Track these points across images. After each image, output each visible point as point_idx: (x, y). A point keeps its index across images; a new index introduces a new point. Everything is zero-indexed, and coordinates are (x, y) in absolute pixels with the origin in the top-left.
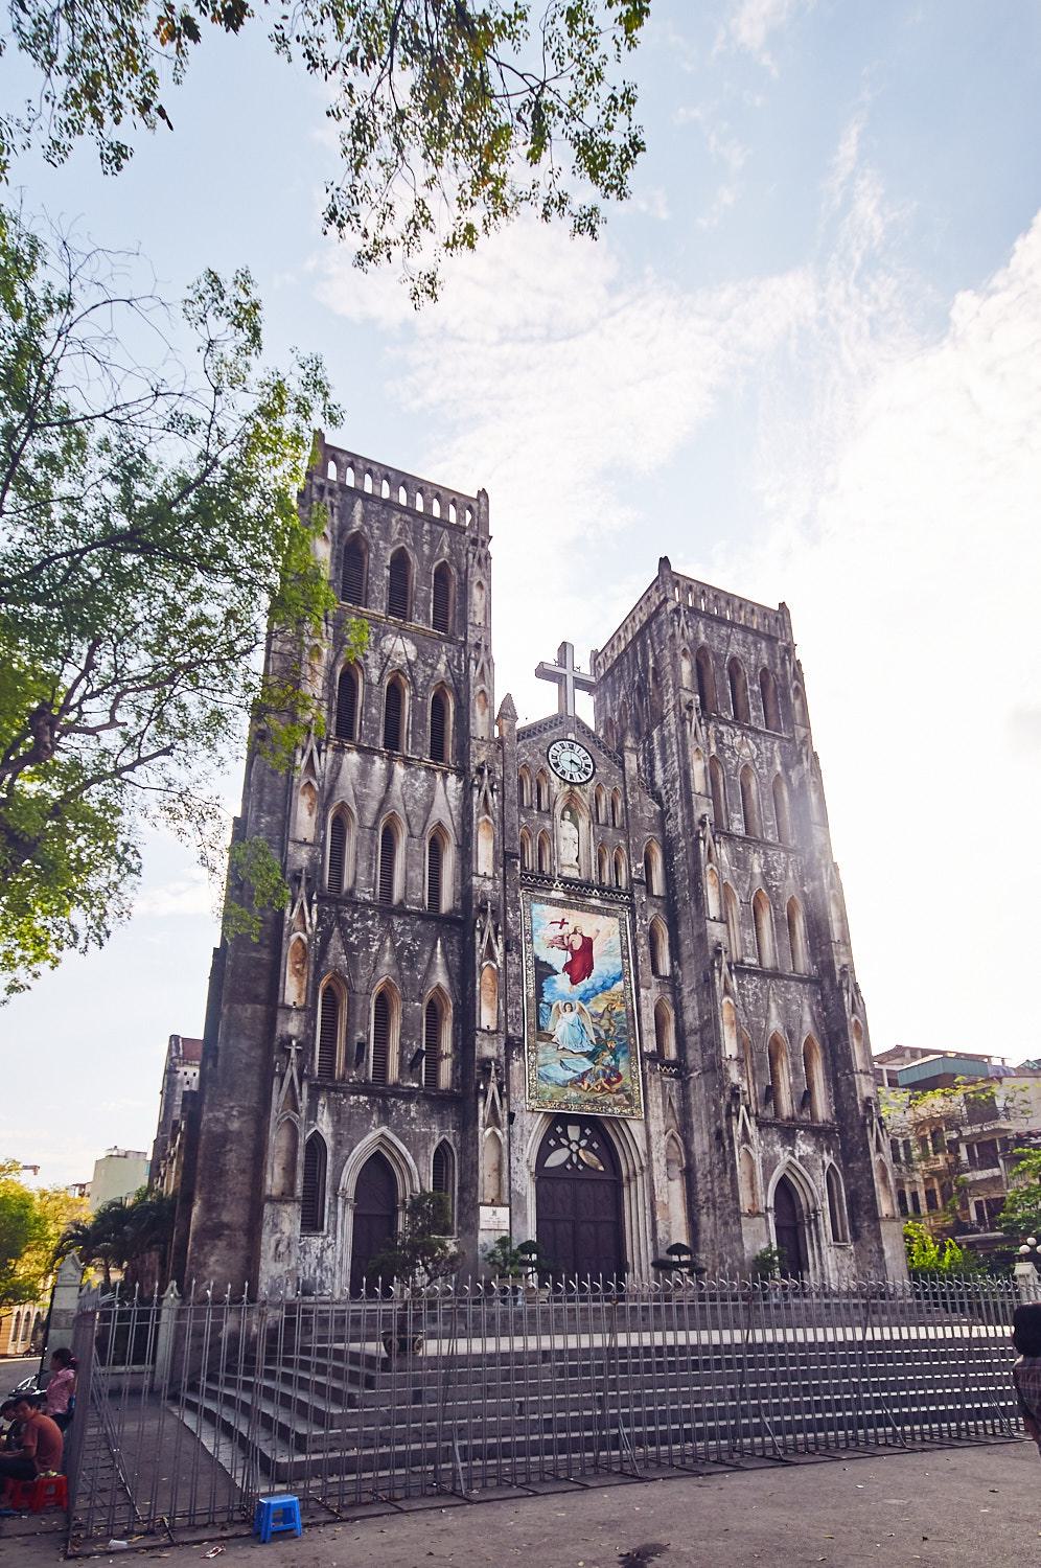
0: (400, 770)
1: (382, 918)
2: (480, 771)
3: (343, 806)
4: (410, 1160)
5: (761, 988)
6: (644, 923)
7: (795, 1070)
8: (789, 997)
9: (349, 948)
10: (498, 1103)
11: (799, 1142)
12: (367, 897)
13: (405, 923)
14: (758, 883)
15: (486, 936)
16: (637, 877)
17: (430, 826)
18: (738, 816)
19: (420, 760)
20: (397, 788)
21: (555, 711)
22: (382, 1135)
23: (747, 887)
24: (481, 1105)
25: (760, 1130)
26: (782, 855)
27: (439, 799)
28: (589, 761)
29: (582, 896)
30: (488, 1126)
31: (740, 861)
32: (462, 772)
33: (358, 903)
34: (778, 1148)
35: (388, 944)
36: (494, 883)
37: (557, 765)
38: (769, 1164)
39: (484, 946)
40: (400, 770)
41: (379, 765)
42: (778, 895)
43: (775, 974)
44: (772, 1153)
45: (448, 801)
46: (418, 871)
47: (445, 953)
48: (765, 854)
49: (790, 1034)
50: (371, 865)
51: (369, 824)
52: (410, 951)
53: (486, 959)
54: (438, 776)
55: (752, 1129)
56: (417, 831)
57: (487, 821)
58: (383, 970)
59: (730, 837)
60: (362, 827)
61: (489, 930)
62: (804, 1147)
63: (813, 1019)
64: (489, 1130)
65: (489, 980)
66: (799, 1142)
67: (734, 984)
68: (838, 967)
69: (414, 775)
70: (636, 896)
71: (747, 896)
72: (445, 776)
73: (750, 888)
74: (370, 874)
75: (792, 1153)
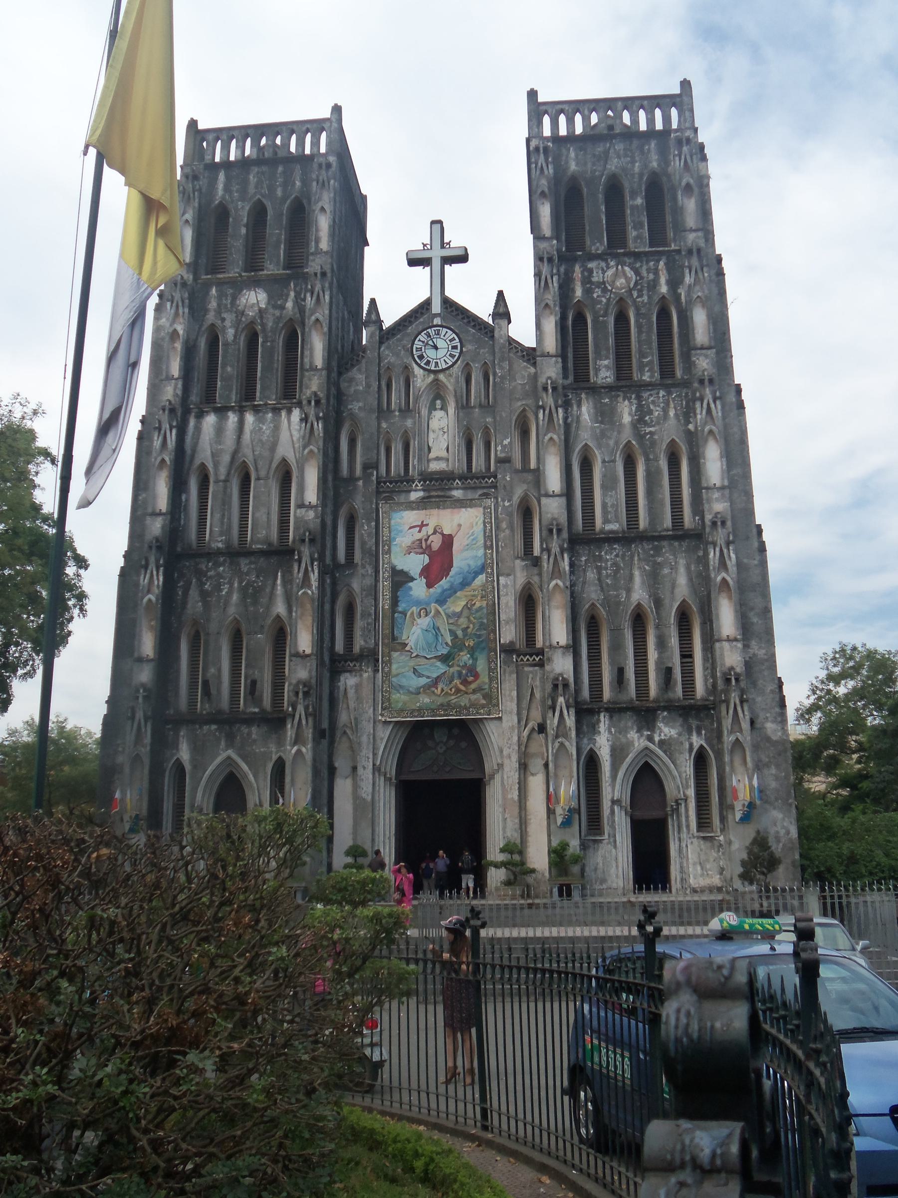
0: (250, 418)
1: (231, 563)
2: (309, 402)
3: (203, 466)
4: (251, 777)
5: (623, 556)
6: (507, 504)
7: (662, 644)
8: (659, 560)
9: (204, 595)
10: (304, 722)
11: (661, 725)
12: (220, 545)
13: (251, 563)
14: (627, 435)
15: (303, 565)
16: (503, 455)
17: (274, 465)
18: (606, 362)
19: (266, 404)
20: (247, 436)
21: (427, 295)
22: (229, 758)
23: (611, 443)
24: (289, 726)
25: (611, 717)
26: (662, 393)
27: (284, 436)
28: (456, 342)
29: (443, 489)
30: (295, 743)
31: (606, 416)
32: (299, 404)
33: (209, 554)
34: (633, 735)
35: (236, 585)
36: (315, 512)
37: (421, 357)
38: (618, 753)
39: (301, 575)
40: (250, 418)
41: (232, 418)
42: (653, 443)
43: (643, 537)
44: (624, 740)
45: (291, 436)
46: (263, 510)
47: (285, 583)
48: (639, 398)
49: (658, 603)
50: (223, 515)
51: (222, 477)
52: (254, 588)
53: (302, 588)
54: (284, 413)
55: (570, 721)
56: (263, 473)
57: (311, 451)
58: (232, 610)
59: (595, 391)
60: (217, 481)
61: (306, 559)
62: (666, 730)
63: (690, 579)
64: (295, 748)
65: (308, 606)
66: (661, 725)
67: (565, 565)
68: (708, 517)
69: (261, 420)
70: (499, 476)
71: (612, 452)
72: (289, 412)
73: (617, 443)
74: (222, 523)
75: (650, 739)
